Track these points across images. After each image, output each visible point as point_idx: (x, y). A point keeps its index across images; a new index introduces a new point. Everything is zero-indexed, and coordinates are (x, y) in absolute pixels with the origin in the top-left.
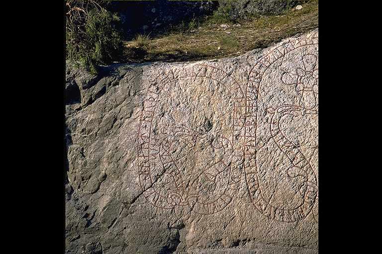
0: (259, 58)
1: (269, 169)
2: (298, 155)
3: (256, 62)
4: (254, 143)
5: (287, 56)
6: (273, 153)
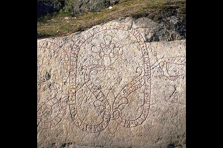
0: (79, 37)
1: (83, 102)
2: (101, 94)
3: (77, 39)
4: (75, 87)
5: (95, 36)
6: (86, 92)
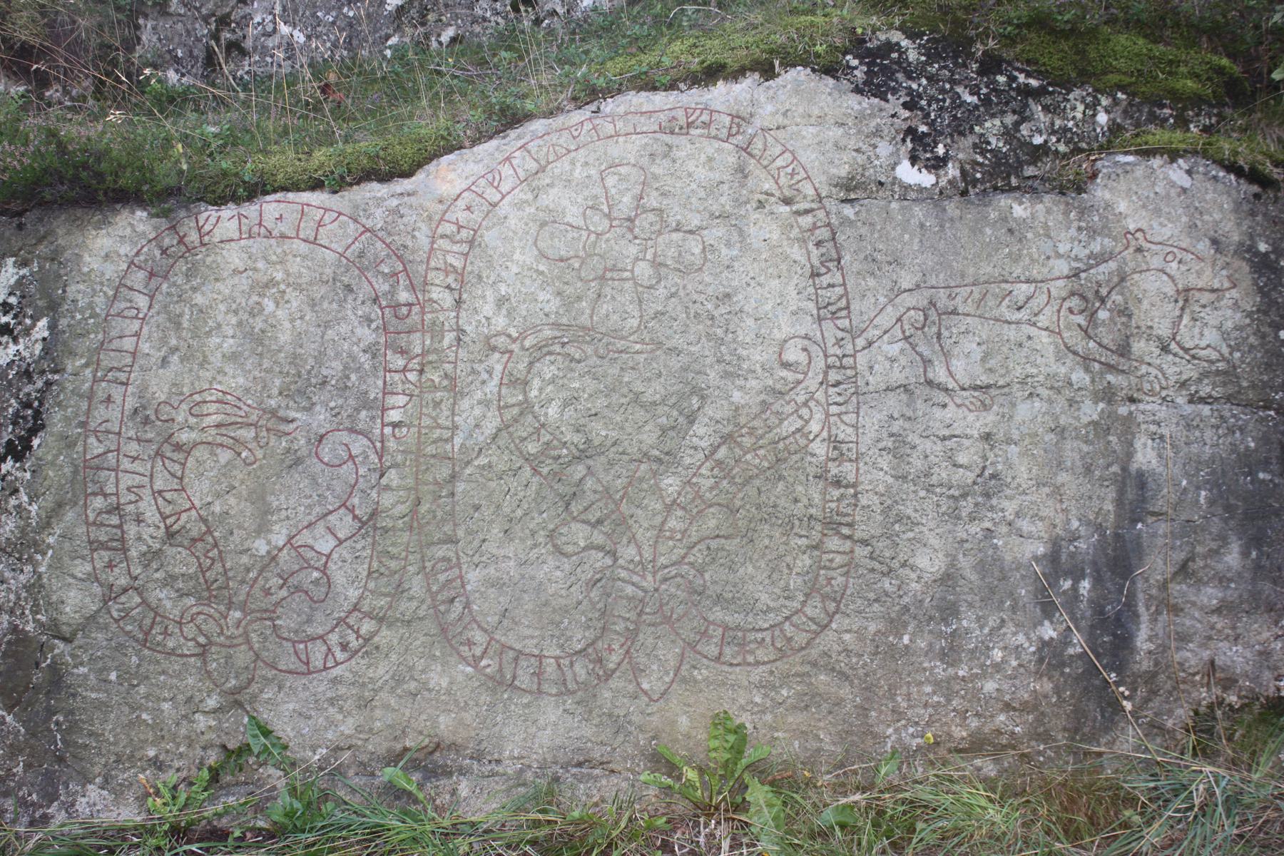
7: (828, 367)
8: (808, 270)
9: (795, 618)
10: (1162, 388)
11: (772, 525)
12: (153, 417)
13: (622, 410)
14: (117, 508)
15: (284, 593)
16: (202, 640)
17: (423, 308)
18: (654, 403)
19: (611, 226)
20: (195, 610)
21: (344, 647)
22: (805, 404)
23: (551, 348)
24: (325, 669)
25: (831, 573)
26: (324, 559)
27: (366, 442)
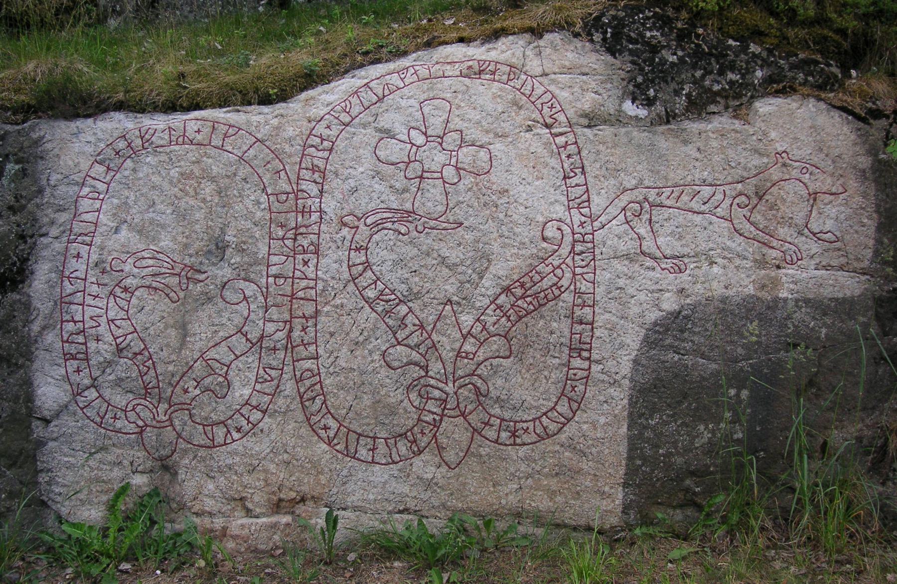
4: (313, 292)
7: (575, 241)
8: (561, 175)
9: (549, 414)
10: (798, 260)
11: (536, 350)
12: (108, 269)
13: (433, 269)
14: (84, 331)
15: (197, 392)
16: (141, 423)
17: (296, 196)
18: (456, 265)
19: (427, 141)
20: (136, 402)
21: (239, 430)
22: (559, 267)
23: (385, 225)
24: (225, 444)
25: (574, 383)
26: (226, 368)
27: (255, 287)
